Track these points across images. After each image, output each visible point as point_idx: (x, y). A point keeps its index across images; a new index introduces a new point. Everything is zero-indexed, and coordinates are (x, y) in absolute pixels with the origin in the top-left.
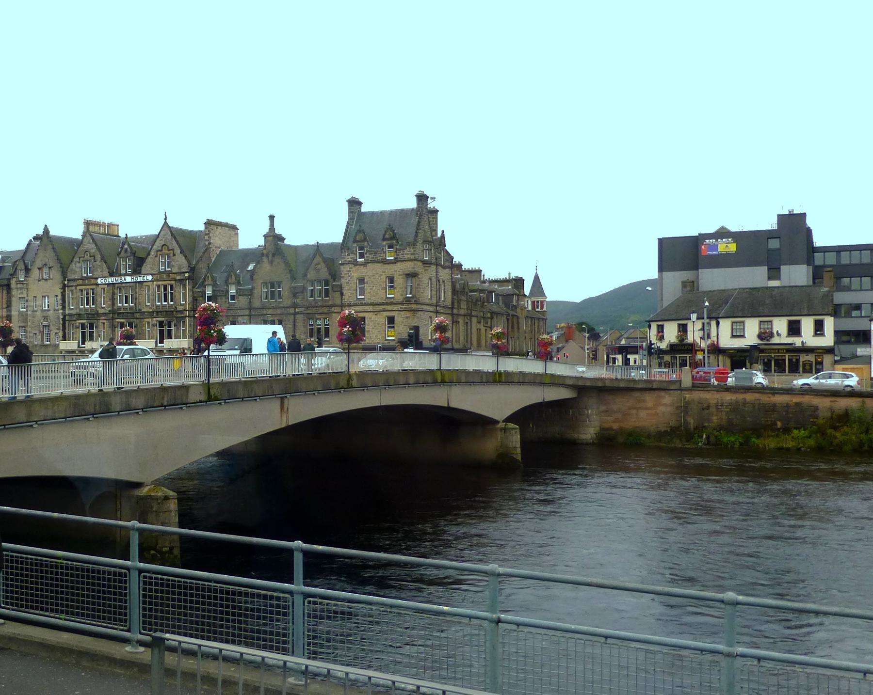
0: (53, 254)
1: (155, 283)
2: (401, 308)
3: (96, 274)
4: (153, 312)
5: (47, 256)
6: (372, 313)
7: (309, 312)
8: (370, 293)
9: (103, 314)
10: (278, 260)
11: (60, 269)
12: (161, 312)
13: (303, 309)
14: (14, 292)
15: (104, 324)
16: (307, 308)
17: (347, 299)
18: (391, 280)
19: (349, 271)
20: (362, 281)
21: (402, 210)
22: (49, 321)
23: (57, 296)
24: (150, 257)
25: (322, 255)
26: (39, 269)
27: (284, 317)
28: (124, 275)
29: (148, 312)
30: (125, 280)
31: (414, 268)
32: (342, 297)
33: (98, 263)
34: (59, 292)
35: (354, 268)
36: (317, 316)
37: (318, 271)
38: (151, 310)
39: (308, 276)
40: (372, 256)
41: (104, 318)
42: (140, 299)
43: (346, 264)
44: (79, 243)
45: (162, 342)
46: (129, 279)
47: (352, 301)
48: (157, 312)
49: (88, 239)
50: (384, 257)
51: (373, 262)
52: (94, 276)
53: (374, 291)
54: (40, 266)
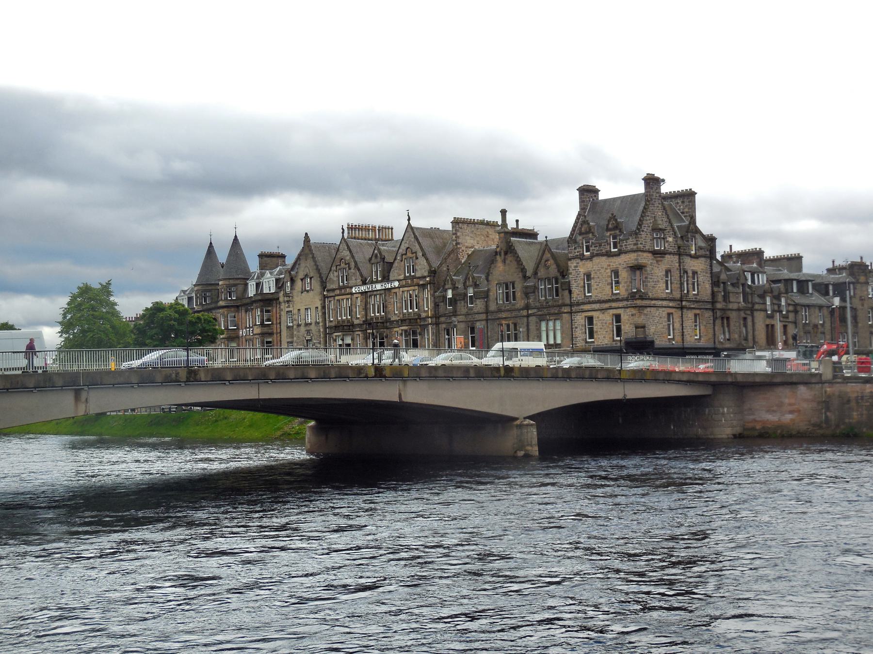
0: (313, 263)
6: (599, 312)
7: (540, 313)
8: (596, 289)
9: (358, 325)
11: (319, 279)
13: (535, 311)
15: (359, 335)
17: (576, 298)
18: (616, 273)
19: (576, 267)
20: (588, 276)
22: (312, 335)
23: (317, 308)
24: (396, 261)
25: (551, 250)
26: (302, 280)
27: (518, 320)
29: (397, 321)
30: (375, 287)
31: (637, 260)
32: (571, 296)
33: (352, 270)
34: (319, 304)
37: (548, 268)
40: (597, 248)
41: (359, 329)
42: (390, 308)
43: (574, 259)
46: (378, 287)
47: (581, 298)
48: (403, 321)
50: (608, 249)
51: (597, 255)
54: (302, 277)
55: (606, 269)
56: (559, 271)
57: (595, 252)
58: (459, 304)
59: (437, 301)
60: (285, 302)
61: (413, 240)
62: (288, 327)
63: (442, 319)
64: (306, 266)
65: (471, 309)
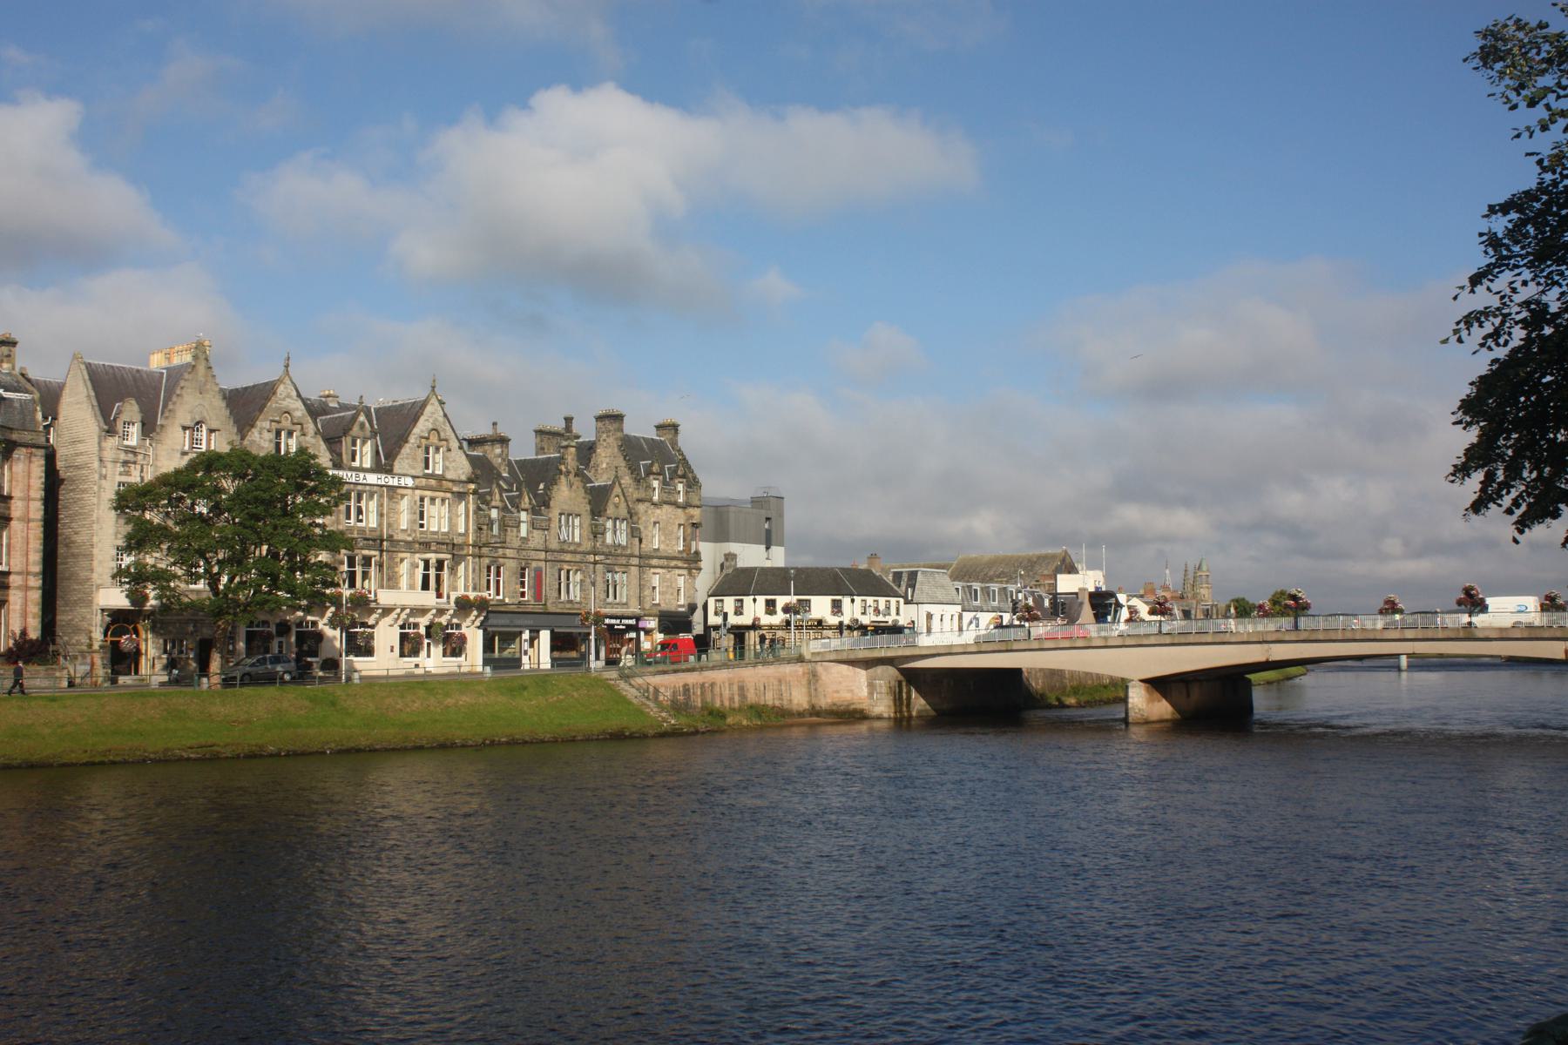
4: (414, 542)
7: (608, 561)
13: (602, 557)
16: (607, 555)
29: (406, 542)
36: (617, 569)
38: (410, 539)
39: (608, 512)
58: (509, 533)
61: (441, 419)
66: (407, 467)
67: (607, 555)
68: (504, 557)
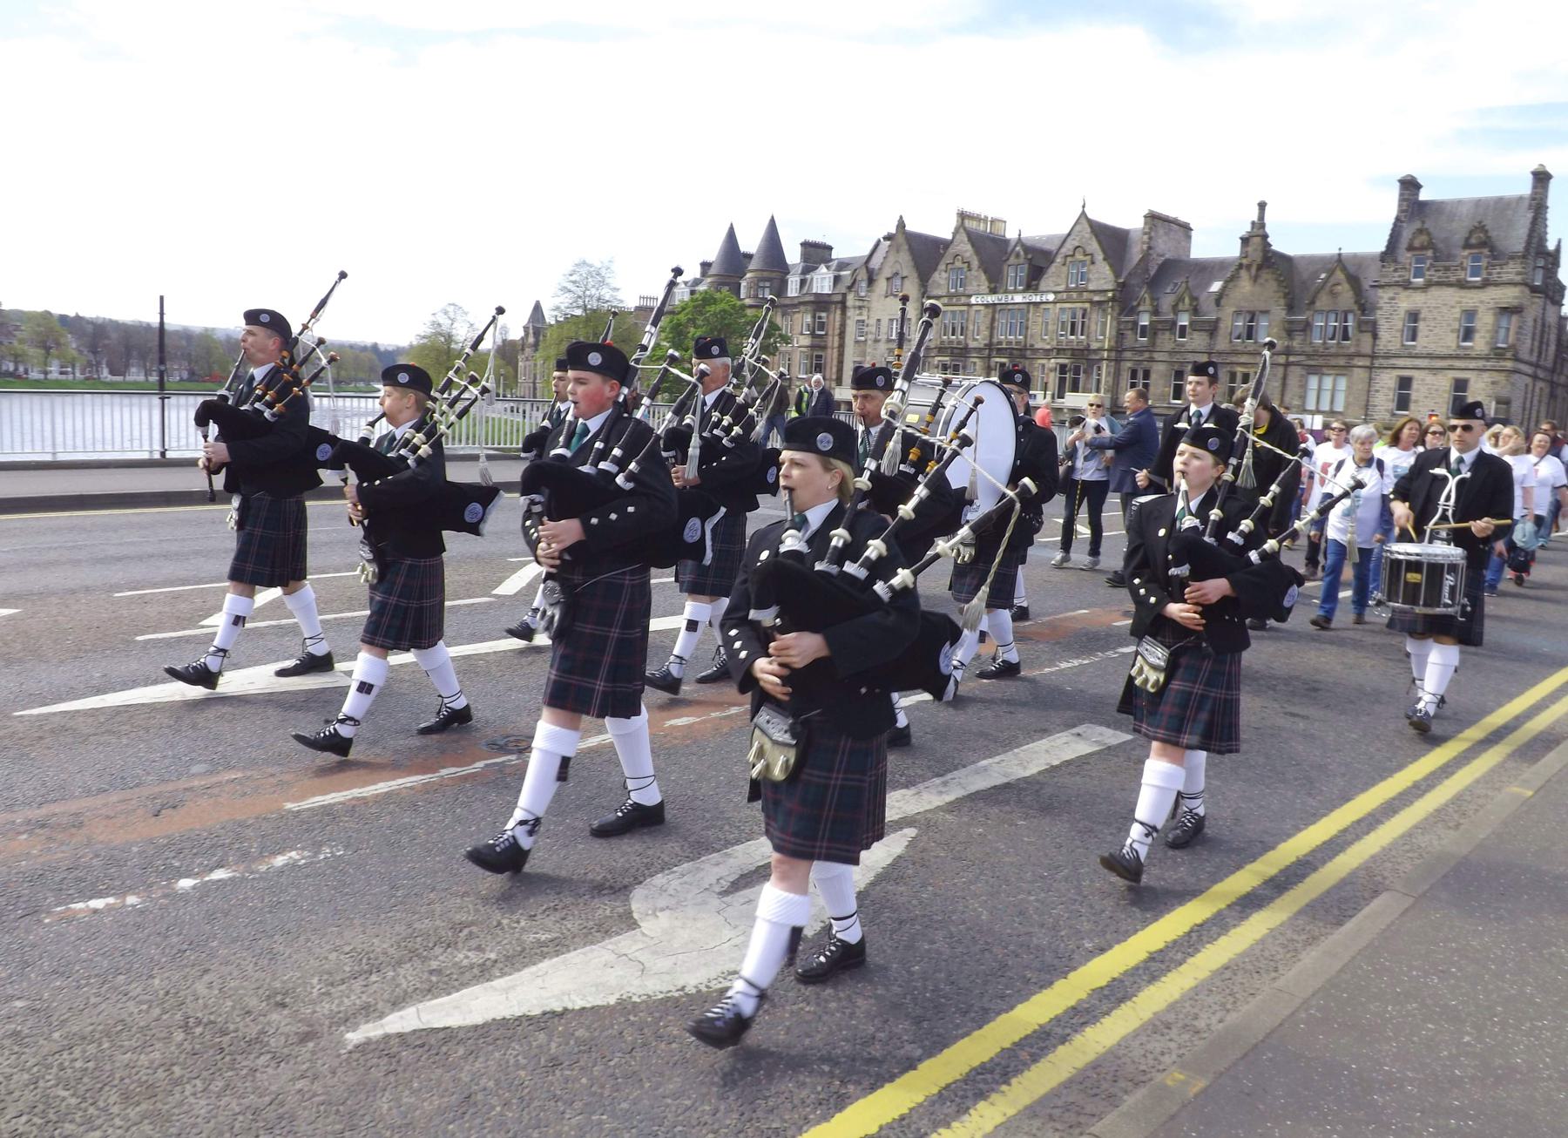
1: (1058, 305)
2: (1484, 366)
3: (970, 290)
5: (904, 262)
6: (1427, 371)
10: (1266, 275)
12: (1064, 350)
13: (1303, 358)
14: (850, 313)
16: (1309, 356)
17: (1385, 346)
19: (1393, 299)
20: (1414, 316)
21: (1499, 200)
26: (888, 279)
28: (1011, 292)
33: (974, 273)
35: (1404, 294)
38: (1048, 347)
40: (1440, 274)
44: (946, 244)
45: (1061, 396)
46: (1018, 298)
47: (1394, 347)
49: (963, 237)
51: (1439, 284)
52: (967, 292)
53: (1436, 335)
54: (889, 276)
55: (1453, 307)
56: (1356, 302)
57: (1435, 279)
58: (1160, 336)
59: (1122, 327)
60: (854, 307)
62: (857, 342)
63: (1128, 355)
64: (897, 262)
65: (1182, 345)
66: (1052, 285)
67: (1309, 356)
68: (1152, 360)
